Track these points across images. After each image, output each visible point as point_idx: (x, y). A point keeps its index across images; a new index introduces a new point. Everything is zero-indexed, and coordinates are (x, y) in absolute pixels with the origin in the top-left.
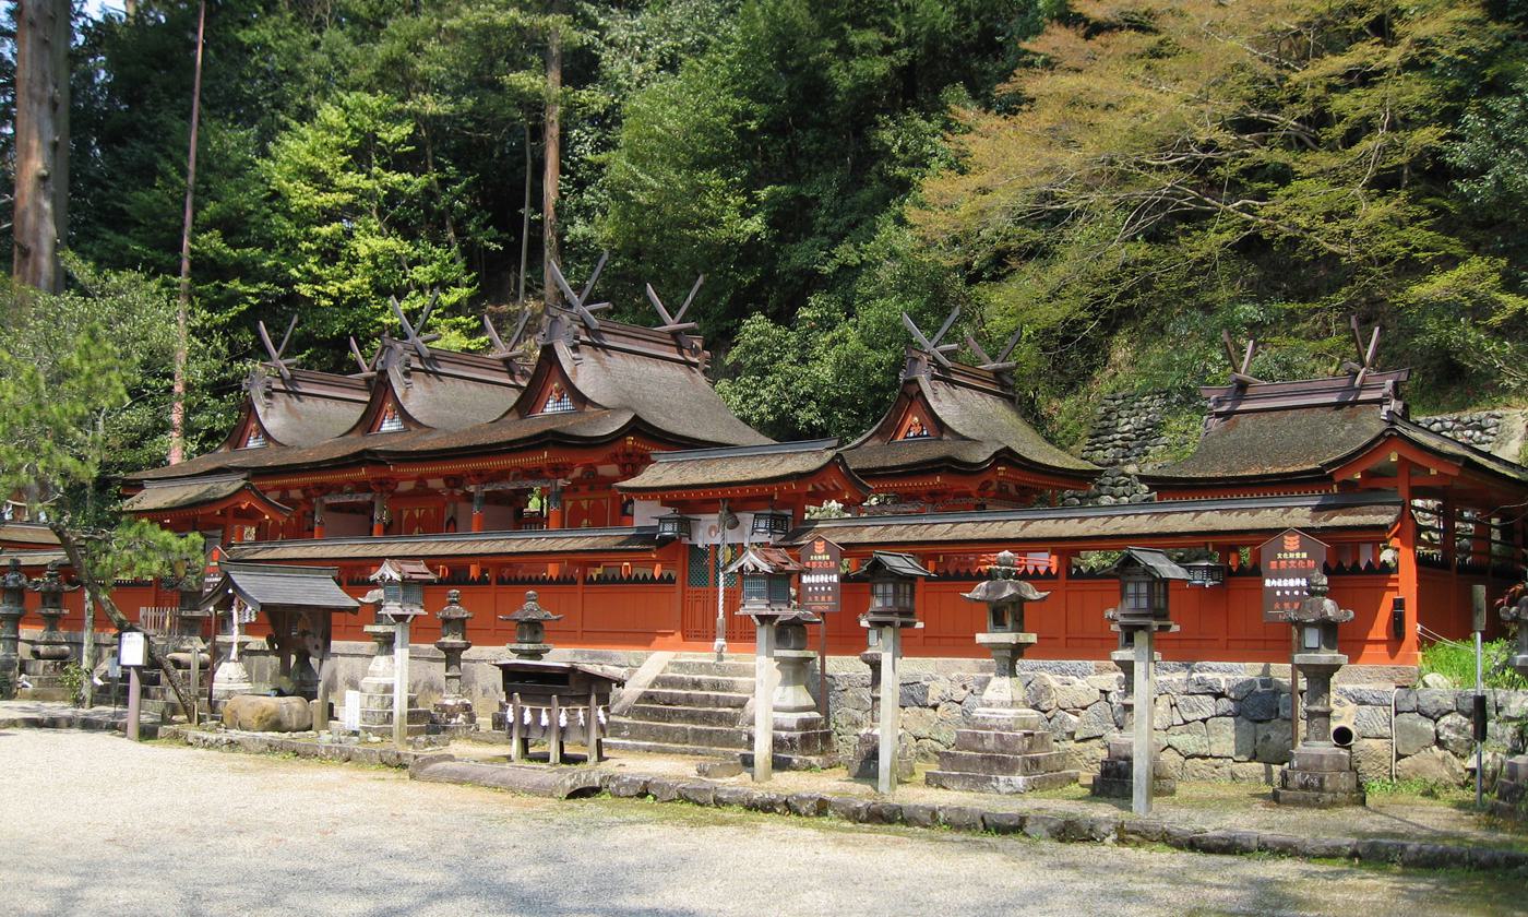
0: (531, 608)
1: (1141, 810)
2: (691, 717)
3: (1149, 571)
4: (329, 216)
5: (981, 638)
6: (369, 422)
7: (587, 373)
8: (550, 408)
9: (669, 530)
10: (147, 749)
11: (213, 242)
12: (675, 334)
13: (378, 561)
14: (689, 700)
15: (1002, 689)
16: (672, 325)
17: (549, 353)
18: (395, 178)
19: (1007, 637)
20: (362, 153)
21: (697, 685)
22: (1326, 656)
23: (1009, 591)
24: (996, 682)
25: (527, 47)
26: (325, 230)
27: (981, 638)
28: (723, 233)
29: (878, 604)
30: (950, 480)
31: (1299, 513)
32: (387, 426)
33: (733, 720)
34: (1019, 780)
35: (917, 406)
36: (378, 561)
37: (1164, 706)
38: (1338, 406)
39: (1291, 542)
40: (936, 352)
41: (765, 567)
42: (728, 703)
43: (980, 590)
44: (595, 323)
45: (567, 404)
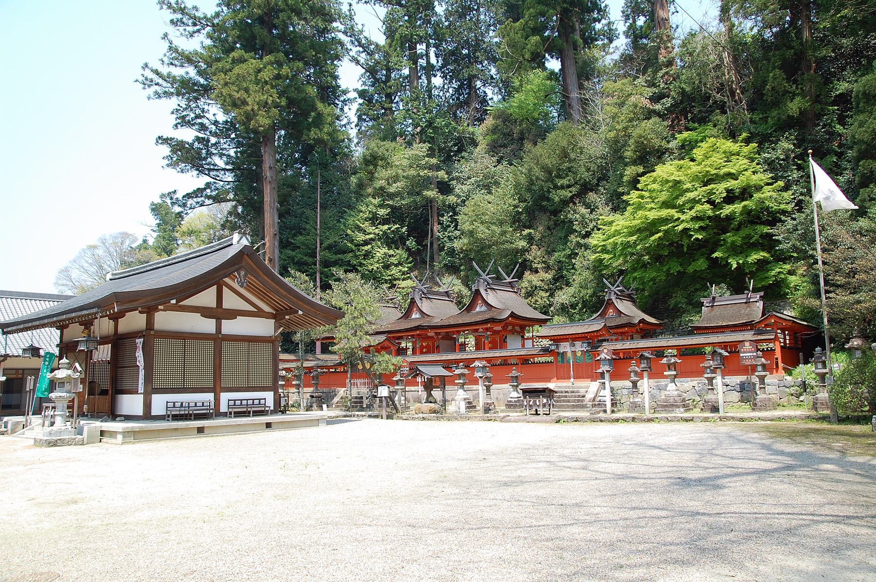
0: (514, 373)
1: (721, 414)
2: (569, 401)
3: (720, 354)
4: (366, 243)
5: (665, 373)
6: (407, 315)
7: (491, 298)
8: (478, 309)
9: (553, 348)
10: (390, 421)
11: (329, 255)
12: (510, 283)
13: (474, 360)
14: (566, 397)
15: (671, 387)
16: (509, 280)
17: (477, 292)
18: (386, 227)
19: (674, 373)
20: (374, 219)
21: (566, 392)
22: (763, 373)
23: (673, 361)
24: (670, 385)
25: (426, 182)
26: (366, 248)
27: (665, 373)
28: (514, 246)
29: (643, 366)
30: (626, 330)
31: (748, 335)
32: (414, 316)
33: (582, 401)
34: (682, 410)
35: (612, 306)
36: (474, 360)
37: (724, 388)
38: (746, 303)
39: (747, 344)
40: (615, 290)
41: (608, 357)
42: (579, 396)
43: (664, 361)
44: (490, 281)
45: (484, 308)
